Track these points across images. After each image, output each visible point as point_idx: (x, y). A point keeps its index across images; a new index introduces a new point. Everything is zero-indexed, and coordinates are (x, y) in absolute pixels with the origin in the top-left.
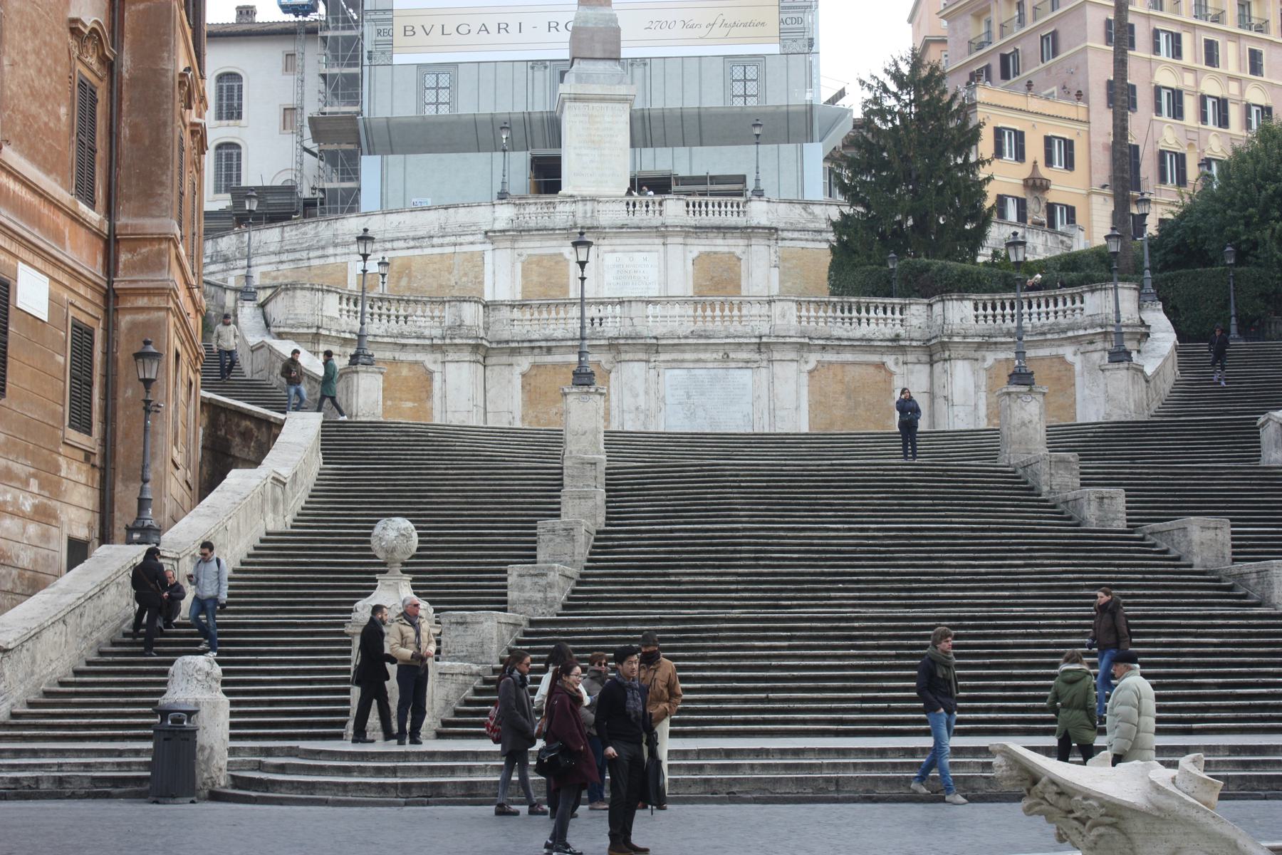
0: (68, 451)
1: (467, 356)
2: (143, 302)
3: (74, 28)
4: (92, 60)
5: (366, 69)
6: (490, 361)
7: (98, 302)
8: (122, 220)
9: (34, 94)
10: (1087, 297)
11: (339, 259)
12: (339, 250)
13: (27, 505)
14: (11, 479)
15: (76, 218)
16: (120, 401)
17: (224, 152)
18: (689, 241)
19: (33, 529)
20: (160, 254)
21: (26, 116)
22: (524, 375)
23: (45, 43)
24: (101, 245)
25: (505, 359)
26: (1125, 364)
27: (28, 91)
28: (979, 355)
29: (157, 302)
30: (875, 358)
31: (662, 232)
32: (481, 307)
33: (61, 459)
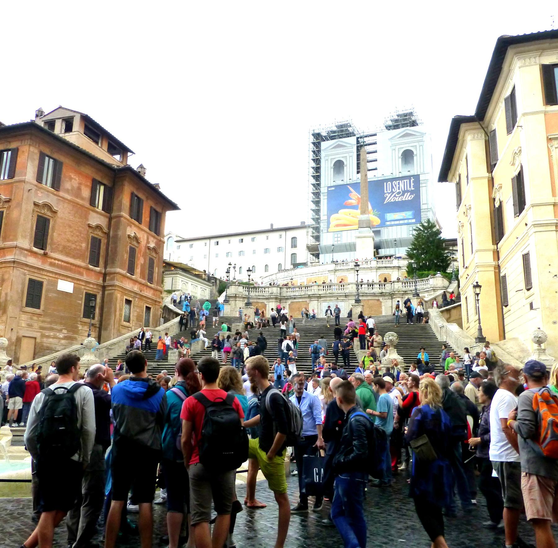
0: (82, 323)
1: (274, 300)
2: (110, 288)
3: (89, 226)
4: (100, 233)
5: (321, 234)
6: (282, 301)
7: (100, 288)
8: (108, 269)
9: (68, 241)
10: (430, 279)
11: (296, 279)
12: (296, 277)
13: (61, 336)
14: (53, 330)
15: (88, 269)
16: (104, 312)
17: (293, 255)
18: (378, 271)
19: (63, 342)
20: (114, 277)
21: (64, 247)
22: (289, 305)
23: (75, 229)
24: (102, 275)
25: (285, 301)
26: (416, 297)
27: (66, 240)
28: (403, 296)
29: (113, 288)
30: (377, 298)
31: (371, 268)
32: (279, 289)
33: (79, 325)
